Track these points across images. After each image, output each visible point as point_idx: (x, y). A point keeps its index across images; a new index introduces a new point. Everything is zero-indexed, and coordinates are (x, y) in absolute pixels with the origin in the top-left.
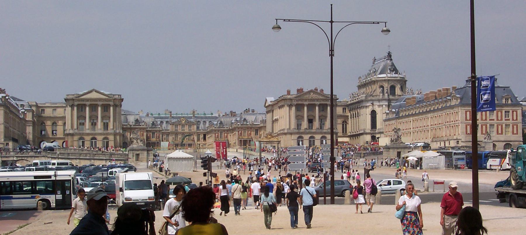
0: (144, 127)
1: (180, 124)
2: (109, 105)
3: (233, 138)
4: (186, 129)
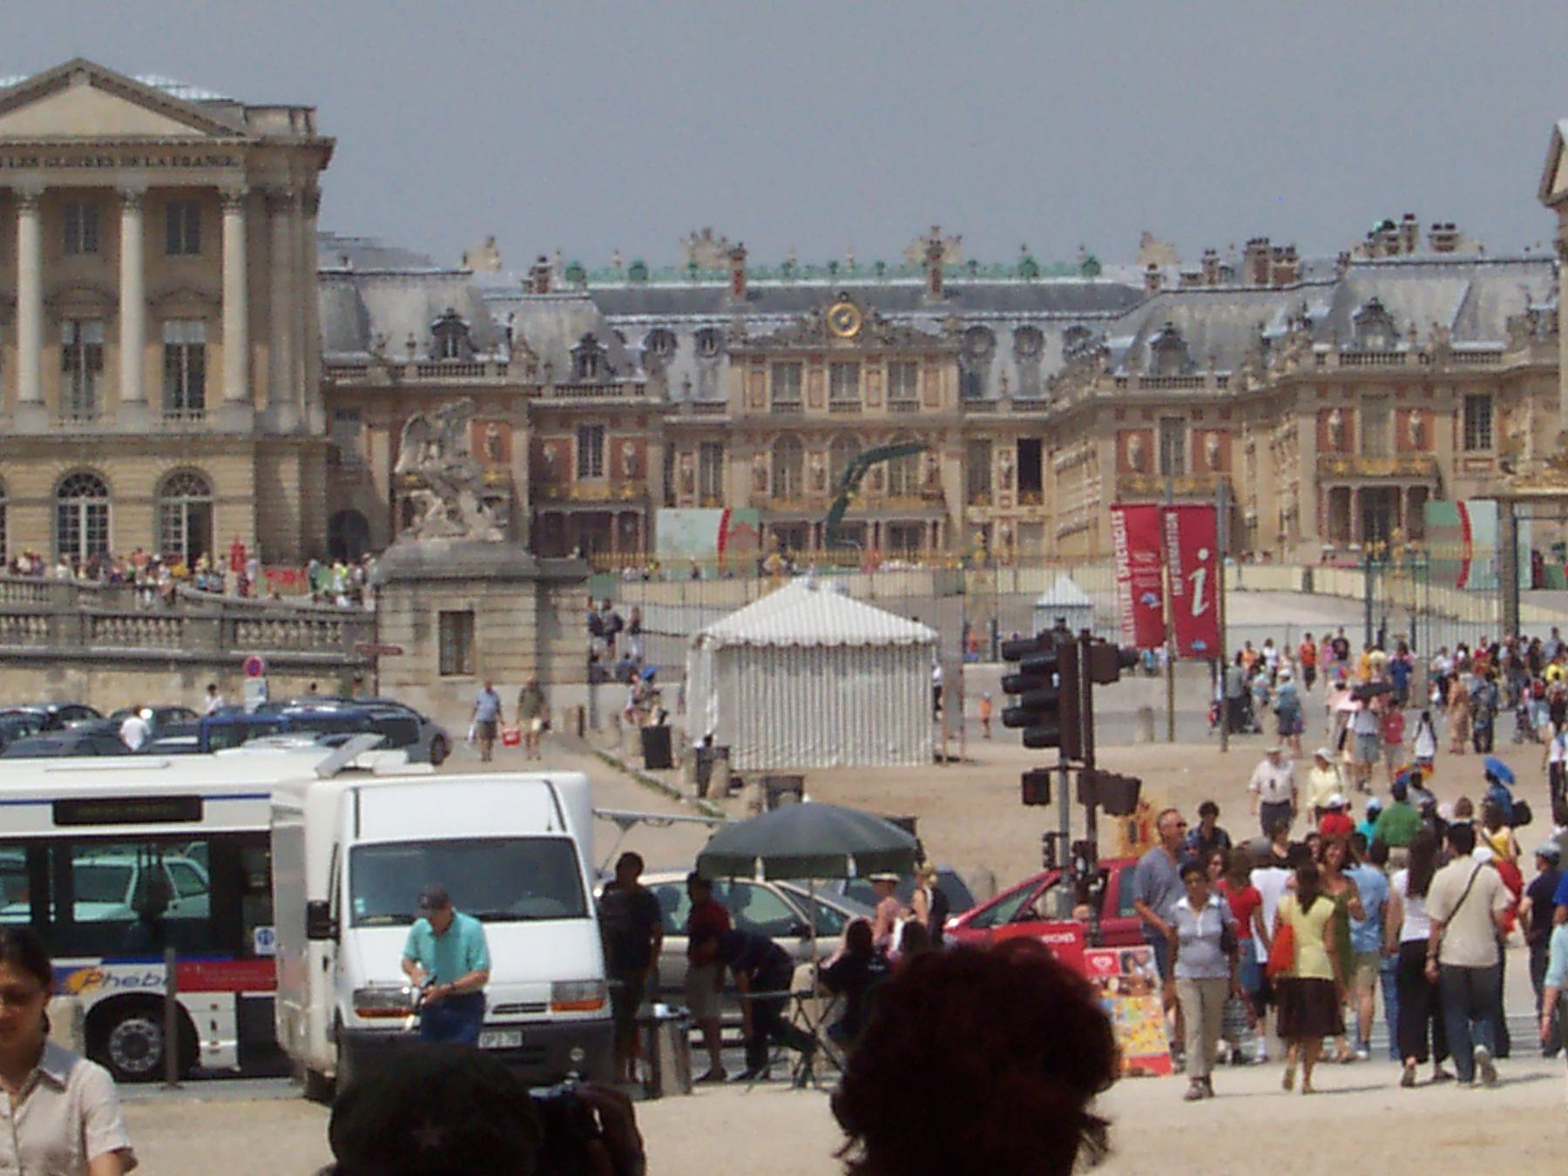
0: (516, 377)
1: (816, 358)
2: (212, 199)
3: (1273, 477)
4: (873, 399)
